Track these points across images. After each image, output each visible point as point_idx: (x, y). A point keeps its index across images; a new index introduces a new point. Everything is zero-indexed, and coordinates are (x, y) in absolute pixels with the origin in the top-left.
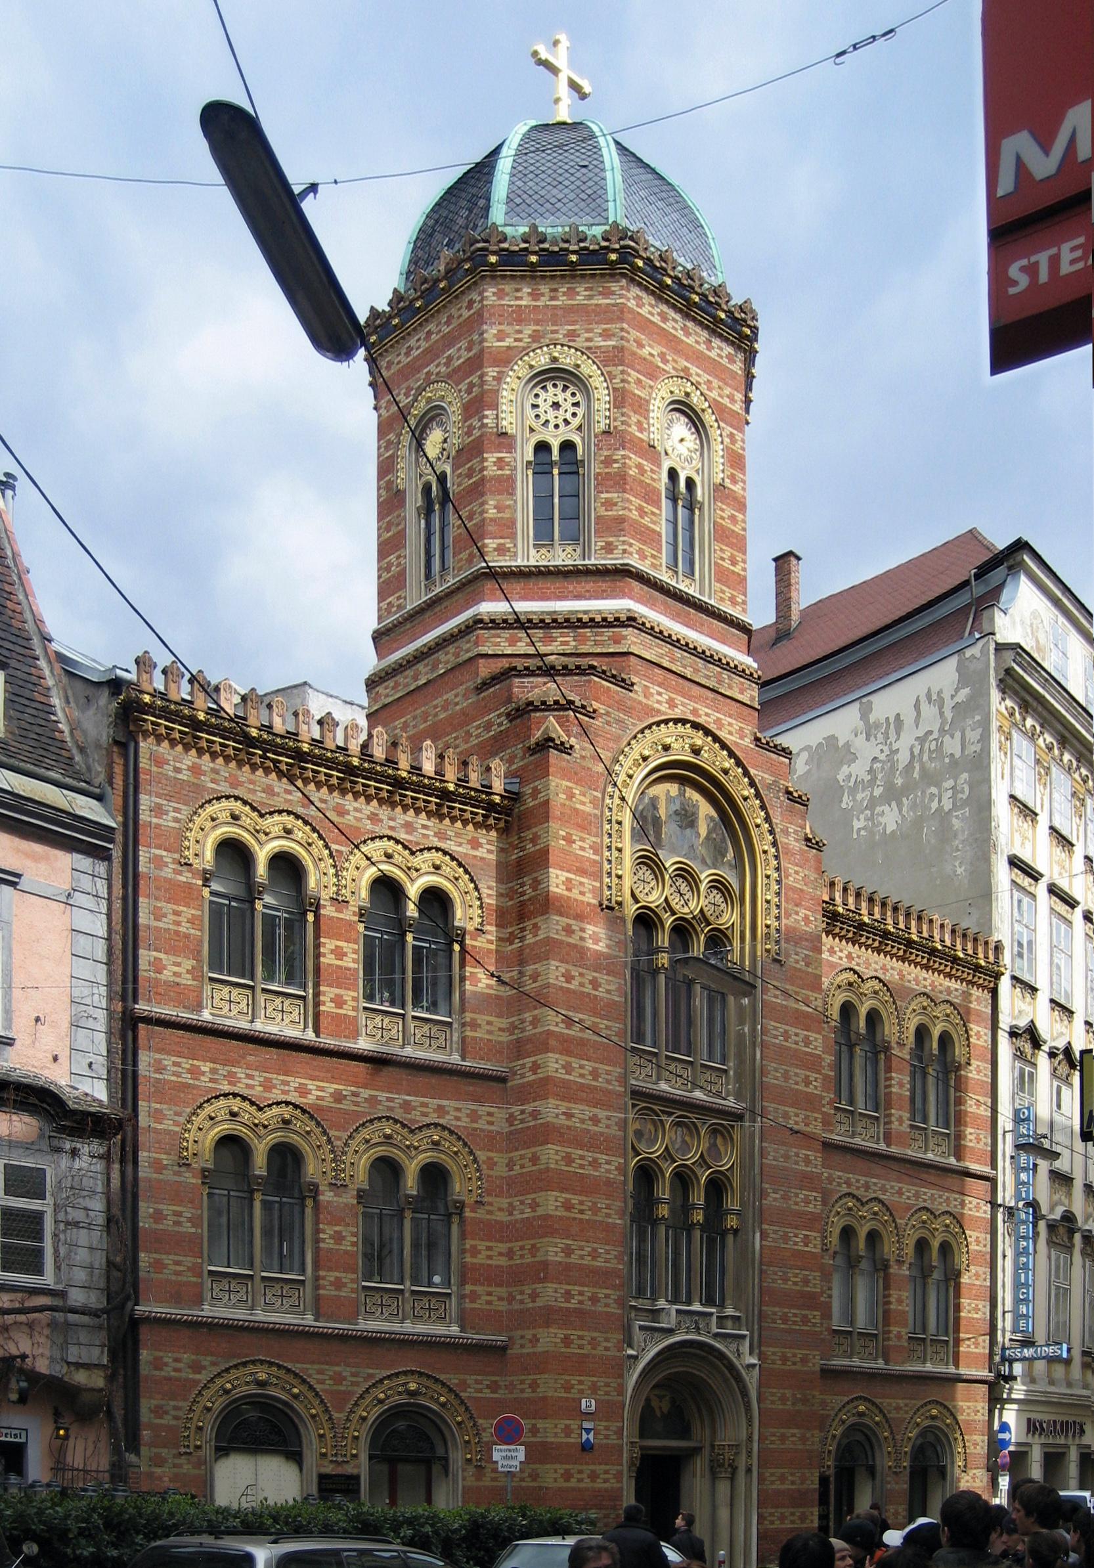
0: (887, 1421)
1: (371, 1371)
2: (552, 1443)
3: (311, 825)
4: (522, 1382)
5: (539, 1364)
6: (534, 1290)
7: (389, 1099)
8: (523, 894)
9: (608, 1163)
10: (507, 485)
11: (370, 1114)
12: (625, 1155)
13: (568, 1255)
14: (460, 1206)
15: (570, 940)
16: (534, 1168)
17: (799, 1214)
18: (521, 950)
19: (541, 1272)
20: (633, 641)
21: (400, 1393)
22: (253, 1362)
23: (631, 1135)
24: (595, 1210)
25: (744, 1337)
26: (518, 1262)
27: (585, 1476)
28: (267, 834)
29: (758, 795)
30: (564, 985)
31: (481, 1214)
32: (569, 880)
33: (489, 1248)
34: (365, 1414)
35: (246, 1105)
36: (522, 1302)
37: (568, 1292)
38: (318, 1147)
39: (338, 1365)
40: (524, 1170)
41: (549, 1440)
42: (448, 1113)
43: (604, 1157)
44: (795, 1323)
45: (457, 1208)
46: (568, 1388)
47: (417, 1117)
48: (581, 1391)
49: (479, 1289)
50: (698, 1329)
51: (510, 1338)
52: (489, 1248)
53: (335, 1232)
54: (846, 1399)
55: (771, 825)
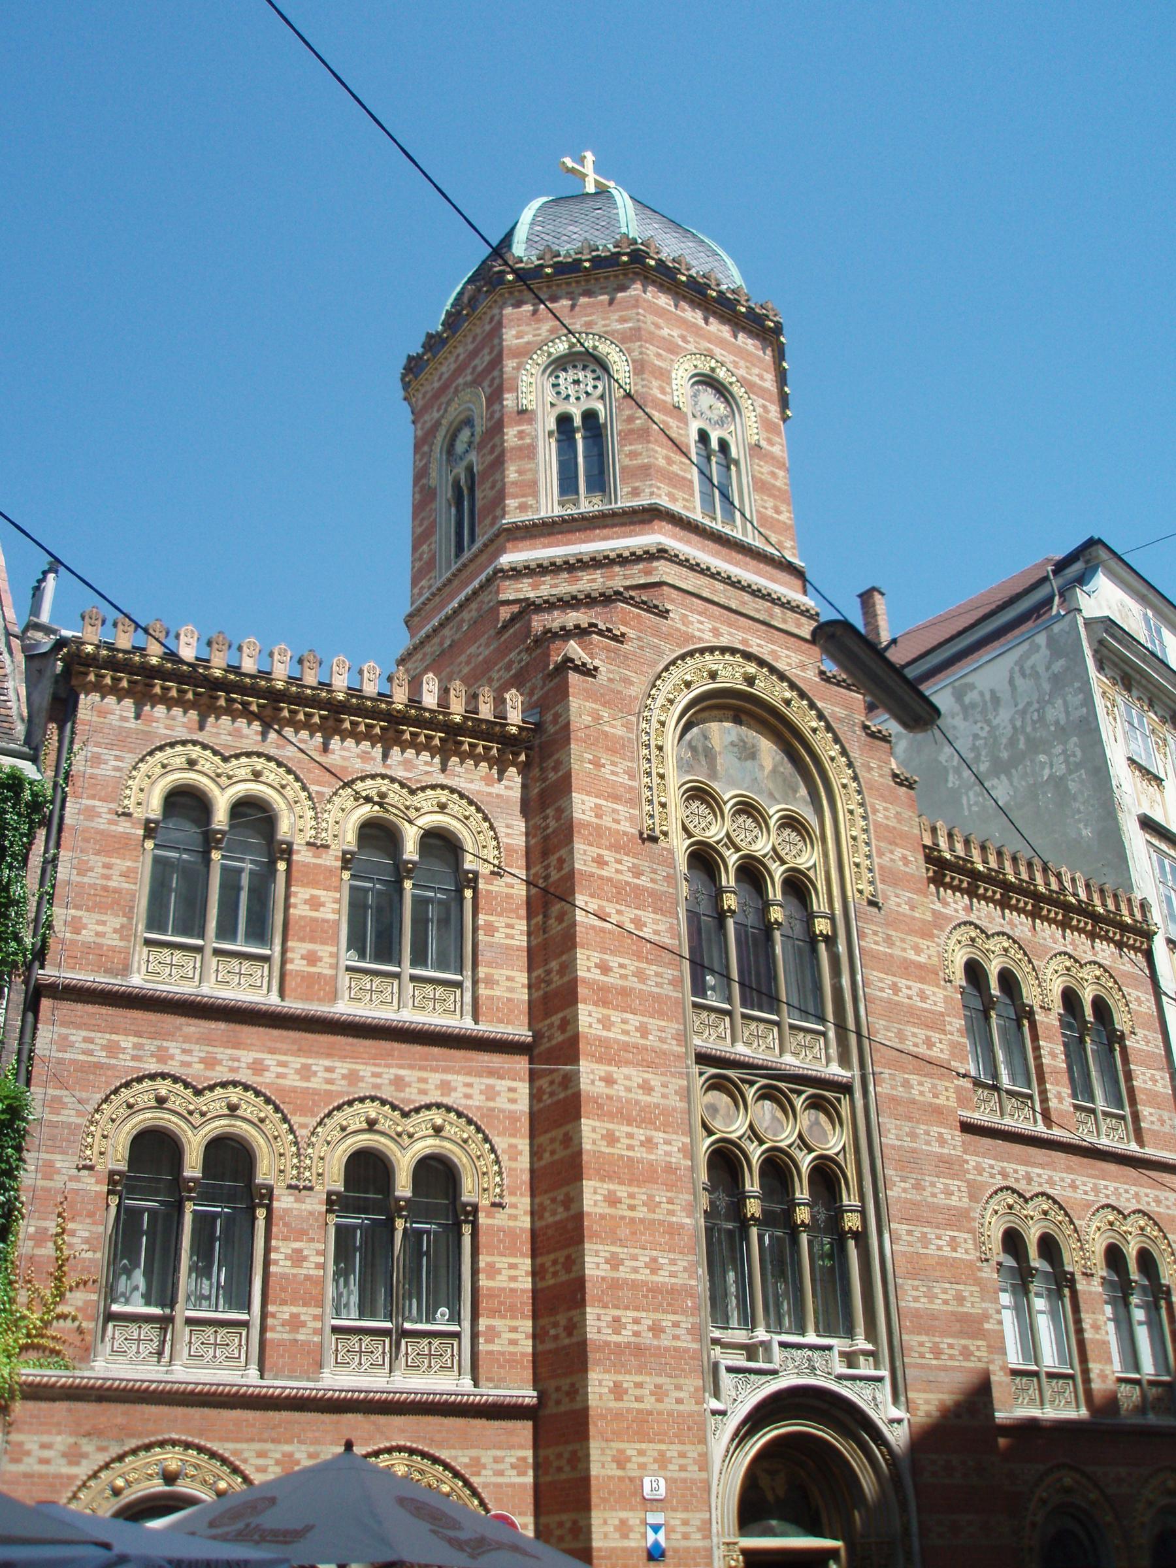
3: (286, 766)
4: (559, 1456)
6: (570, 1319)
7: (375, 1075)
8: (547, 827)
10: (529, 452)
11: (348, 1093)
12: (691, 1133)
13: (615, 1267)
15: (604, 873)
20: (664, 571)
22: (162, 1444)
24: (652, 1205)
25: (880, 1379)
28: (229, 777)
29: (829, 728)
31: (500, 1219)
32: (598, 806)
35: (179, 1087)
36: (556, 1337)
38: (276, 1138)
39: (289, 1441)
40: (556, 1157)
42: (455, 1089)
43: (661, 1135)
44: (952, 1357)
46: (621, 1461)
47: (412, 1096)
48: (642, 1466)
49: (497, 1323)
53: (294, 1251)
55: (848, 757)
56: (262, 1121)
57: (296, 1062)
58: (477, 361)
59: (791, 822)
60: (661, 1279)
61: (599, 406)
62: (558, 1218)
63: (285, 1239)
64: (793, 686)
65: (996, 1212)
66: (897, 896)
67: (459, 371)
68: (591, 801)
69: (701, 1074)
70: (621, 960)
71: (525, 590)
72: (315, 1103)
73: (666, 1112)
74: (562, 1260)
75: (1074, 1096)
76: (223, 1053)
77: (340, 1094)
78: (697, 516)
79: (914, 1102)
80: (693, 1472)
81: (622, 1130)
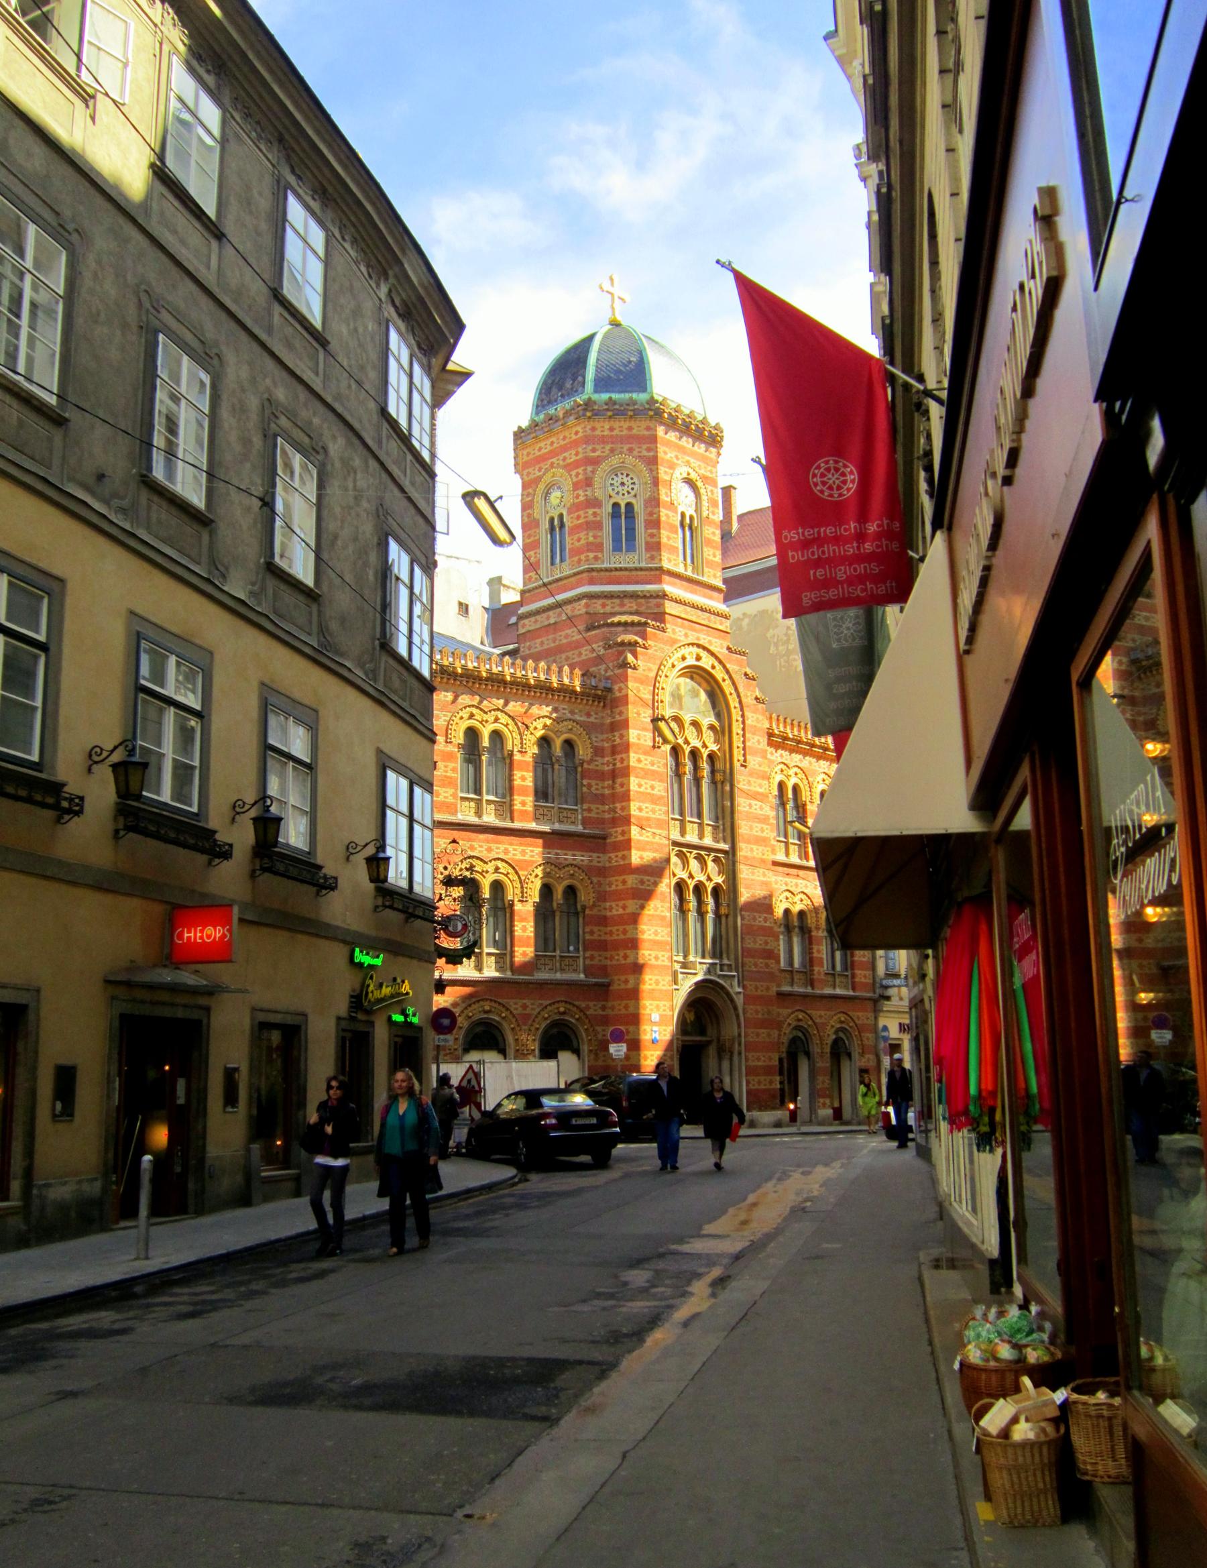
14: (584, 908)
15: (641, 766)
18: (613, 771)
58: (566, 454)
61: (633, 501)
64: (716, 658)
67: (553, 454)
71: (597, 606)
76: (494, 846)
78: (680, 569)
81: (646, 878)
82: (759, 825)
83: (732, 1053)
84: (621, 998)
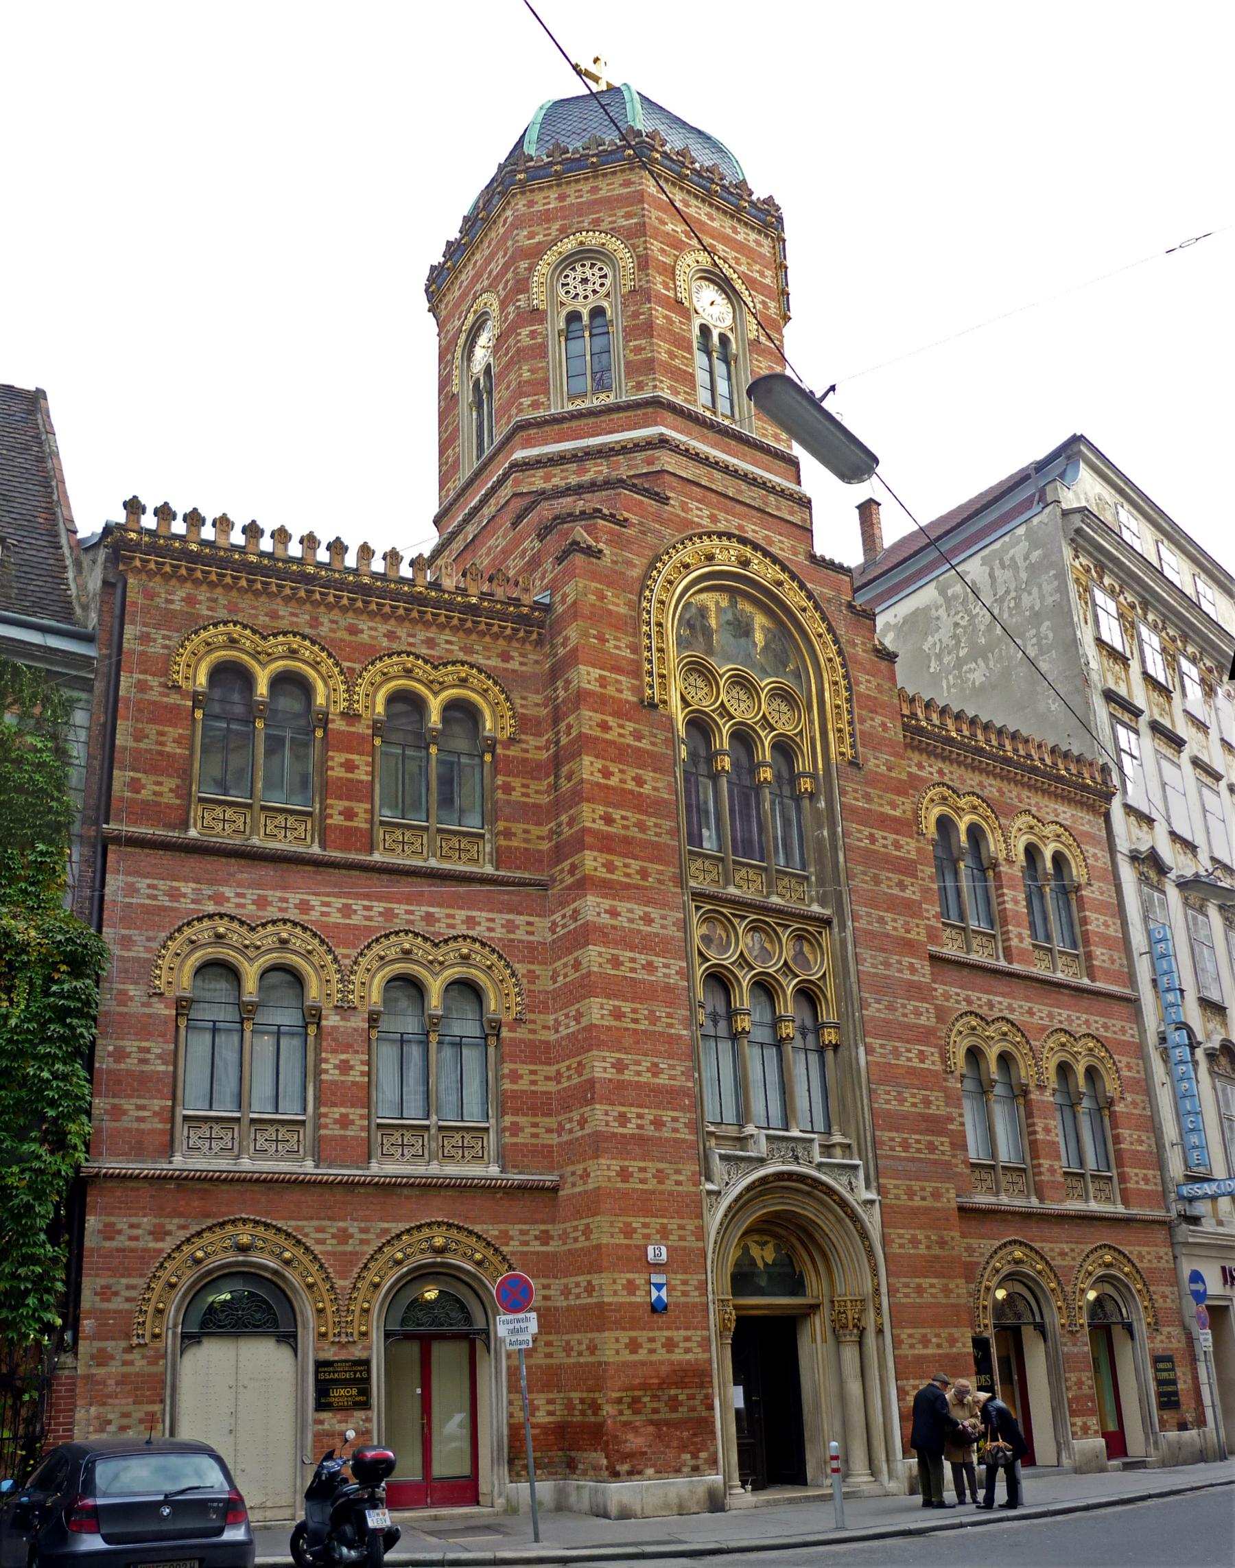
0: (1051, 1269)
1: (386, 1225)
2: (610, 1304)
4: (575, 1229)
5: (592, 1203)
6: (582, 1115)
8: (557, 697)
9: (666, 966)
11: (384, 928)
12: (687, 957)
14: (496, 1026)
15: (608, 736)
16: (577, 975)
17: (909, 1027)
18: (556, 755)
19: (587, 1093)
21: (422, 1251)
23: (697, 941)
25: (855, 1167)
26: (566, 1085)
27: (658, 1345)
30: (602, 781)
31: (521, 1033)
33: (533, 1072)
34: (377, 1279)
36: (571, 1131)
37: (622, 1115)
38: (322, 967)
39: (344, 1220)
40: (568, 979)
41: (606, 1300)
42: (479, 924)
43: (661, 960)
44: (919, 1151)
45: (494, 1028)
46: (628, 1232)
48: (647, 1237)
49: (522, 1120)
50: (797, 1158)
51: (561, 1177)
52: (533, 1072)
54: (997, 1243)
56: (310, 952)
57: (338, 902)
59: (780, 694)
60: (661, 1081)
62: (570, 1030)
63: (334, 1051)
65: (961, 1033)
66: (876, 758)
68: (596, 672)
69: (698, 908)
70: (624, 813)
72: (356, 937)
73: (665, 941)
74: (575, 1065)
75: (1034, 935)
77: (378, 929)
79: (887, 935)
80: (691, 1242)
82: (896, 877)
83: (862, 1332)
84: (578, 1214)
